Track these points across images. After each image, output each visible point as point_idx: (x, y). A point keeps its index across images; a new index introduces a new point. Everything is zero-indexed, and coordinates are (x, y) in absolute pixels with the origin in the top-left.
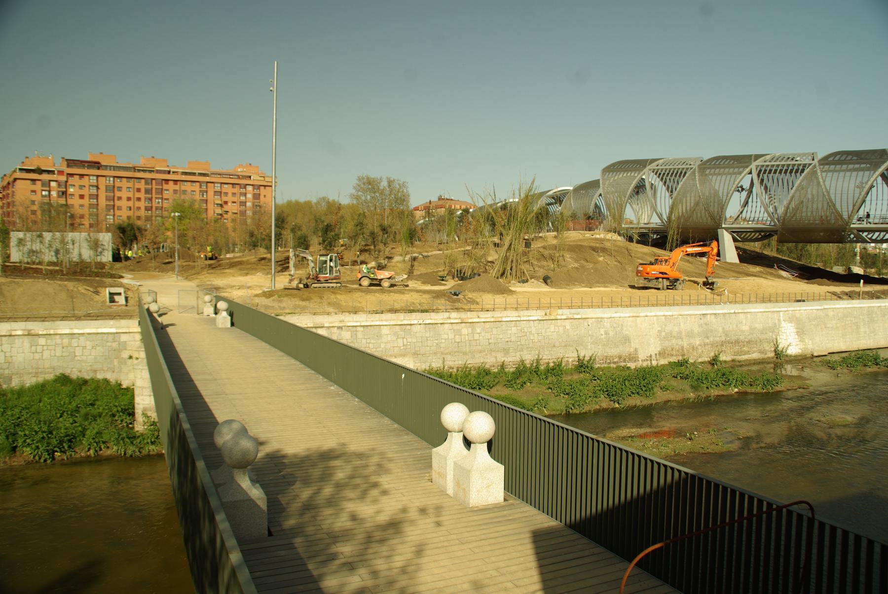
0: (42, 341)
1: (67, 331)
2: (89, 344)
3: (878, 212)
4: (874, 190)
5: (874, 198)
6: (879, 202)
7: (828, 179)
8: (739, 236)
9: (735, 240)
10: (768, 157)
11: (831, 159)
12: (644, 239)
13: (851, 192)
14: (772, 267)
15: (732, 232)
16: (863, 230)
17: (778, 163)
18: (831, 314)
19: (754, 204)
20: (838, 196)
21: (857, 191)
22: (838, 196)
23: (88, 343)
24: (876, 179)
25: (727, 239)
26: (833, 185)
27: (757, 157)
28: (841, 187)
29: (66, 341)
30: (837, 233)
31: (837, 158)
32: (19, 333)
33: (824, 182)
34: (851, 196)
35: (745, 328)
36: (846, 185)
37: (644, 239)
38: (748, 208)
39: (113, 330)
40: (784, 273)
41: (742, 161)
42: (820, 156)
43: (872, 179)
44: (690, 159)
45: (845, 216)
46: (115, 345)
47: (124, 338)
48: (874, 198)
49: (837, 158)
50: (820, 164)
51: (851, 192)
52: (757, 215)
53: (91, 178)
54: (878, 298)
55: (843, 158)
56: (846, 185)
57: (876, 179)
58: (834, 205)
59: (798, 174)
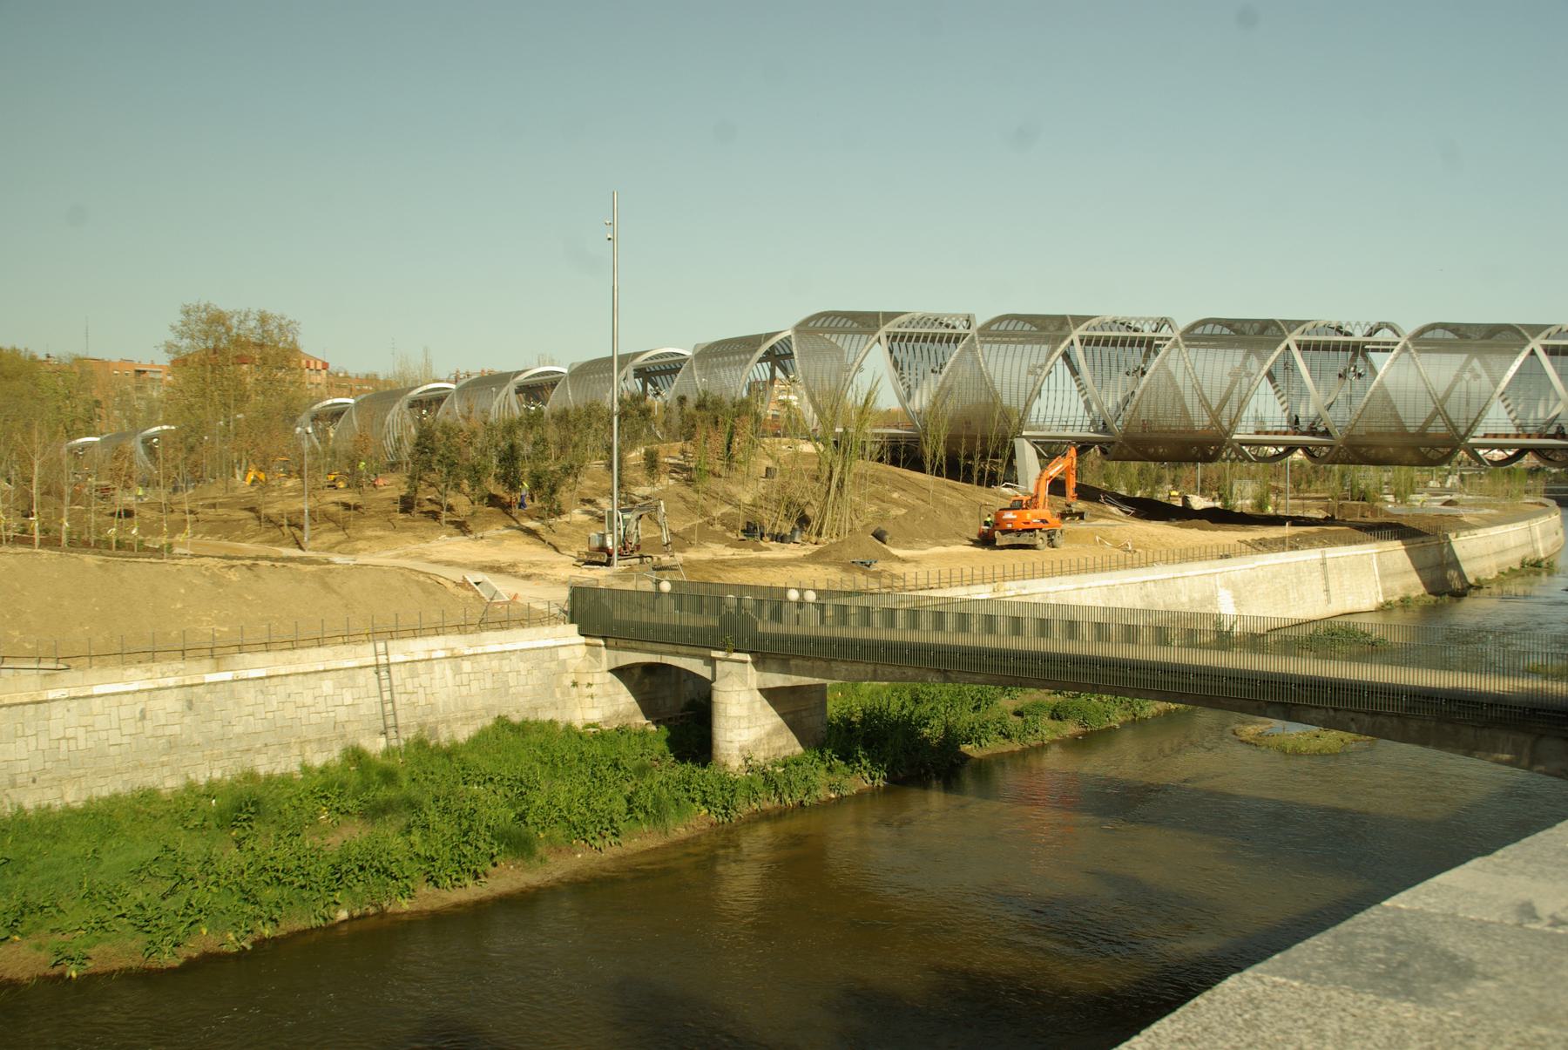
0: (466, 666)
1: (499, 648)
3: (1058, 413)
4: (1052, 376)
5: (1052, 386)
6: (1060, 394)
8: (1049, 450)
9: (1040, 455)
10: (1094, 322)
11: (994, 327)
12: (904, 453)
13: (1023, 380)
14: (1097, 500)
16: (1243, 443)
17: (918, 330)
18: (1261, 573)
19: (1052, 394)
20: (1006, 387)
21: (1031, 378)
22: (1006, 387)
23: (522, 665)
25: (1027, 457)
28: (1006, 369)
29: (495, 663)
30: (1200, 448)
31: (1002, 327)
32: (441, 654)
33: (986, 364)
34: (1022, 388)
35: (1184, 599)
36: (1016, 365)
37: (904, 453)
38: (1061, 404)
39: (551, 643)
40: (1114, 509)
41: (865, 323)
42: (980, 321)
44: (950, 316)
45: (1226, 424)
46: (553, 665)
47: (563, 654)
48: (1052, 386)
50: (981, 335)
51: (1023, 380)
54: (1293, 548)
55: (1019, 327)
56: (1016, 365)
58: (1182, 398)
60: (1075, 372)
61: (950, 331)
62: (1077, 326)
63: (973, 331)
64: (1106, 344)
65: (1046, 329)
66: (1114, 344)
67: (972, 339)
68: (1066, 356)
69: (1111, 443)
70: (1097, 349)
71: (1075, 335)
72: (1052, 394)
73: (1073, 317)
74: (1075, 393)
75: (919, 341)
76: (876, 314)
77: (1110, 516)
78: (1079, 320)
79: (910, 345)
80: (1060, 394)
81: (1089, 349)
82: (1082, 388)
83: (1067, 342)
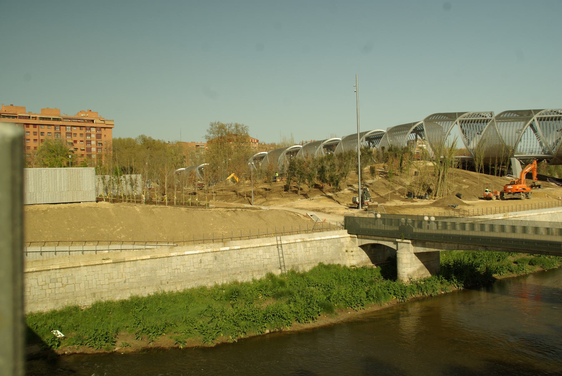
0: (308, 245)
1: (319, 238)
2: (328, 245)
4: (526, 133)
6: (529, 140)
7: (501, 128)
8: (525, 162)
10: (543, 112)
11: (502, 116)
12: (468, 164)
13: (514, 136)
14: (546, 180)
15: (520, 159)
17: (471, 119)
19: (526, 140)
20: (507, 138)
21: (517, 134)
24: (527, 129)
25: (517, 165)
26: (504, 131)
27: (460, 114)
28: (507, 132)
29: (318, 244)
31: (505, 116)
32: (299, 241)
33: (499, 130)
37: (468, 164)
38: (530, 144)
39: (338, 236)
40: (553, 184)
41: (451, 117)
42: (496, 114)
43: (525, 129)
44: (484, 113)
47: (342, 240)
49: (505, 116)
51: (514, 136)
52: (528, 147)
53: (67, 128)
55: (512, 115)
57: (527, 129)
59: (485, 123)
60: (535, 131)
61: (484, 118)
62: (535, 114)
63: (493, 118)
64: (548, 120)
65: (523, 115)
66: (552, 120)
67: (493, 121)
68: (531, 126)
69: (551, 158)
70: (544, 122)
71: (535, 117)
72: (526, 140)
73: (534, 110)
74: (535, 140)
75: (472, 123)
76: (455, 114)
77: (552, 186)
78: (536, 111)
79: (469, 124)
80: (529, 140)
81: (541, 122)
82: (538, 137)
83: (532, 120)
